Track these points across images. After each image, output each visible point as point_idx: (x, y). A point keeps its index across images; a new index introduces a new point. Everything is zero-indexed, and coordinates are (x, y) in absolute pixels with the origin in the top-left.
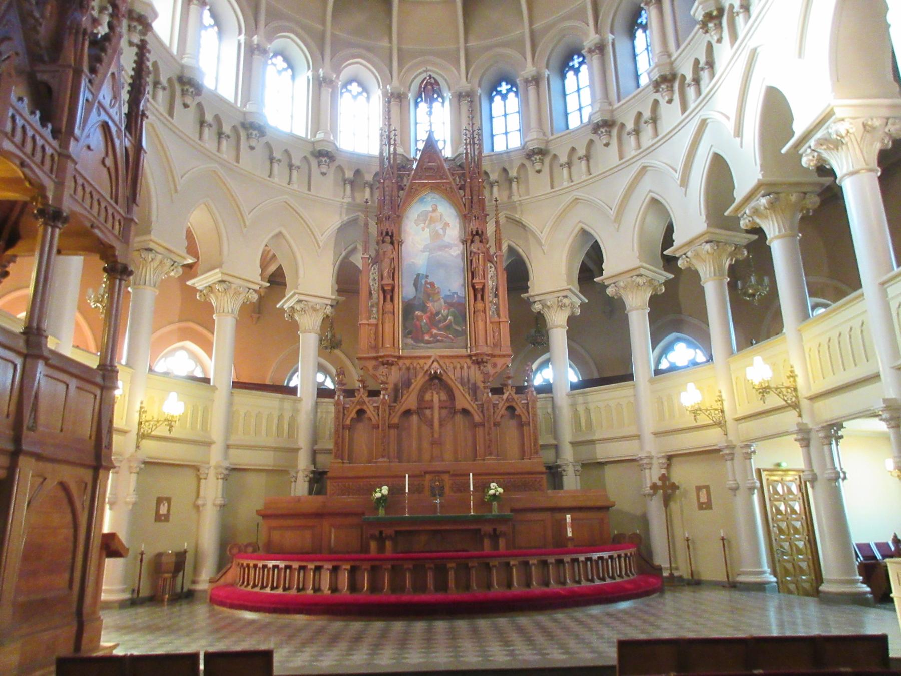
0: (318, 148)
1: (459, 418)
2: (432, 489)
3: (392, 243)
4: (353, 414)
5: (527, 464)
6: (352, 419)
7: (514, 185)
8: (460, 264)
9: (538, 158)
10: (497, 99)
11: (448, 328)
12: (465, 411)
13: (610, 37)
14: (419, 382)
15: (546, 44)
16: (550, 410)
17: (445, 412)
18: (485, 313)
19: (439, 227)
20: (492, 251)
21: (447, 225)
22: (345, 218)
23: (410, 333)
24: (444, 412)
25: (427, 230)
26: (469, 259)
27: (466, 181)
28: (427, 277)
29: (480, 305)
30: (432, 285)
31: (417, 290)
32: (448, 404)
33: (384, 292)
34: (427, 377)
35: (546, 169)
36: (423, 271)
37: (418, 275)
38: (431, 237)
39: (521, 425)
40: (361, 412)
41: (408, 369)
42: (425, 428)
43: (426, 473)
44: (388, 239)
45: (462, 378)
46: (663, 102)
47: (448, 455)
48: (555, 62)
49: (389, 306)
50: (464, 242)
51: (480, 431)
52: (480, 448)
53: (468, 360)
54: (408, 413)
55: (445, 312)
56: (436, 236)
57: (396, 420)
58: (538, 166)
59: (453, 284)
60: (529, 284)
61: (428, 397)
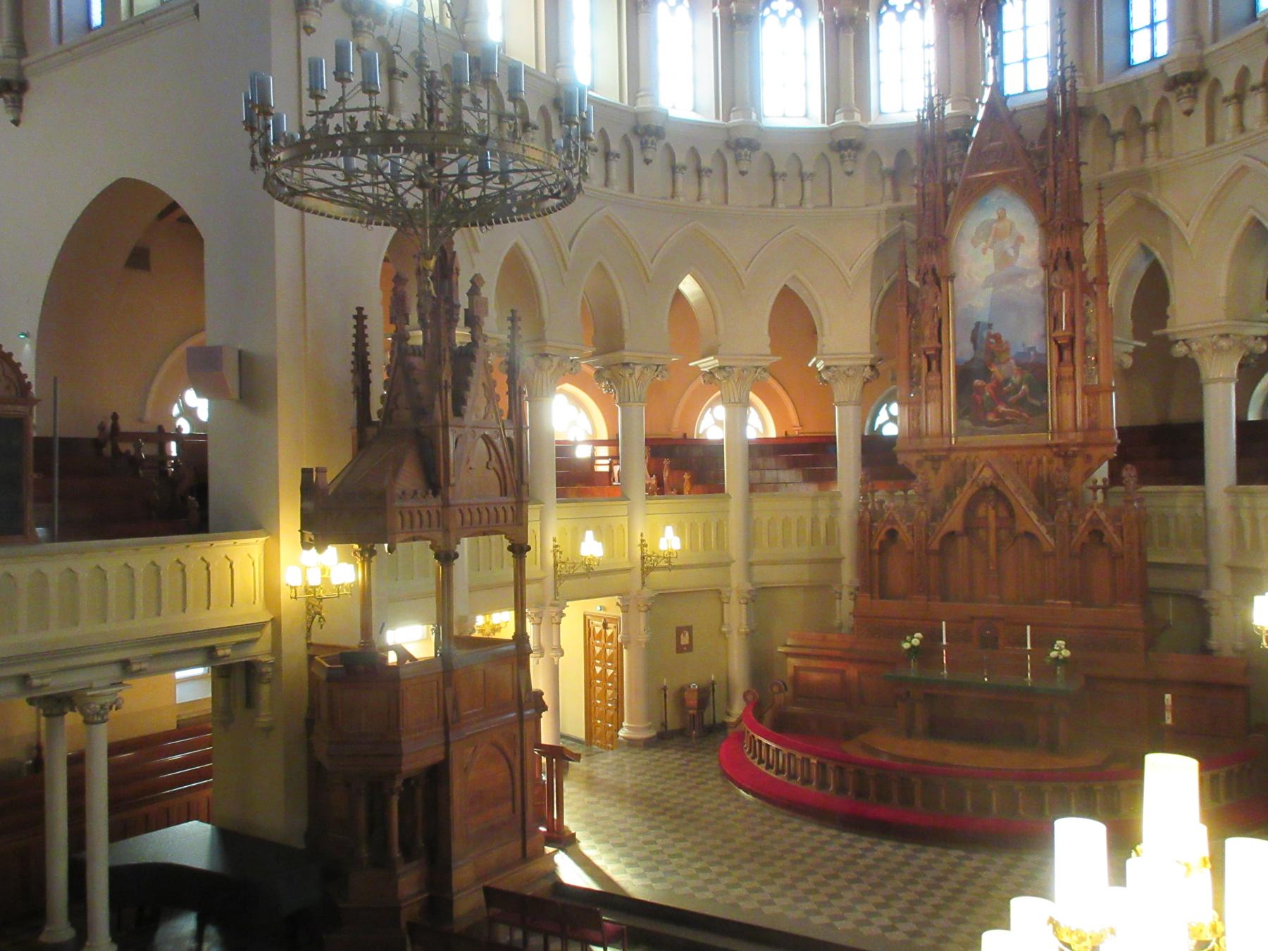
4: (882, 536)
6: (881, 543)
7: (1150, 137)
8: (1040, 299)
9: (1184, 89)
11: (1021, 402)
12: (1028, 535)
16: (1200, 512)
17: (1003, 533)
18: (1074, 378)
19: (1008, 245)
21: (1020, 239)
25: (990, 252)
26: (1050, 292)
28: (990, 326)
29: (1067, 371)
30: (997, 338)
31: (975, 348)
33: (928, 357)
34: (975, 489)
35: (1201, 107)
36: (984, 319)
37: (978, 324)
38: (997, 261)
41: (965, 464)
43: (973, 618)
44: (930, 278)
50: (1045, 266)
53: (1048, 451)
54: (951, 535)
55: (1016, 379)
56: (1003, 260)
58: (1186, 105)
59: (1026, 335)
60: (1169, 312)
61: (981, 511)
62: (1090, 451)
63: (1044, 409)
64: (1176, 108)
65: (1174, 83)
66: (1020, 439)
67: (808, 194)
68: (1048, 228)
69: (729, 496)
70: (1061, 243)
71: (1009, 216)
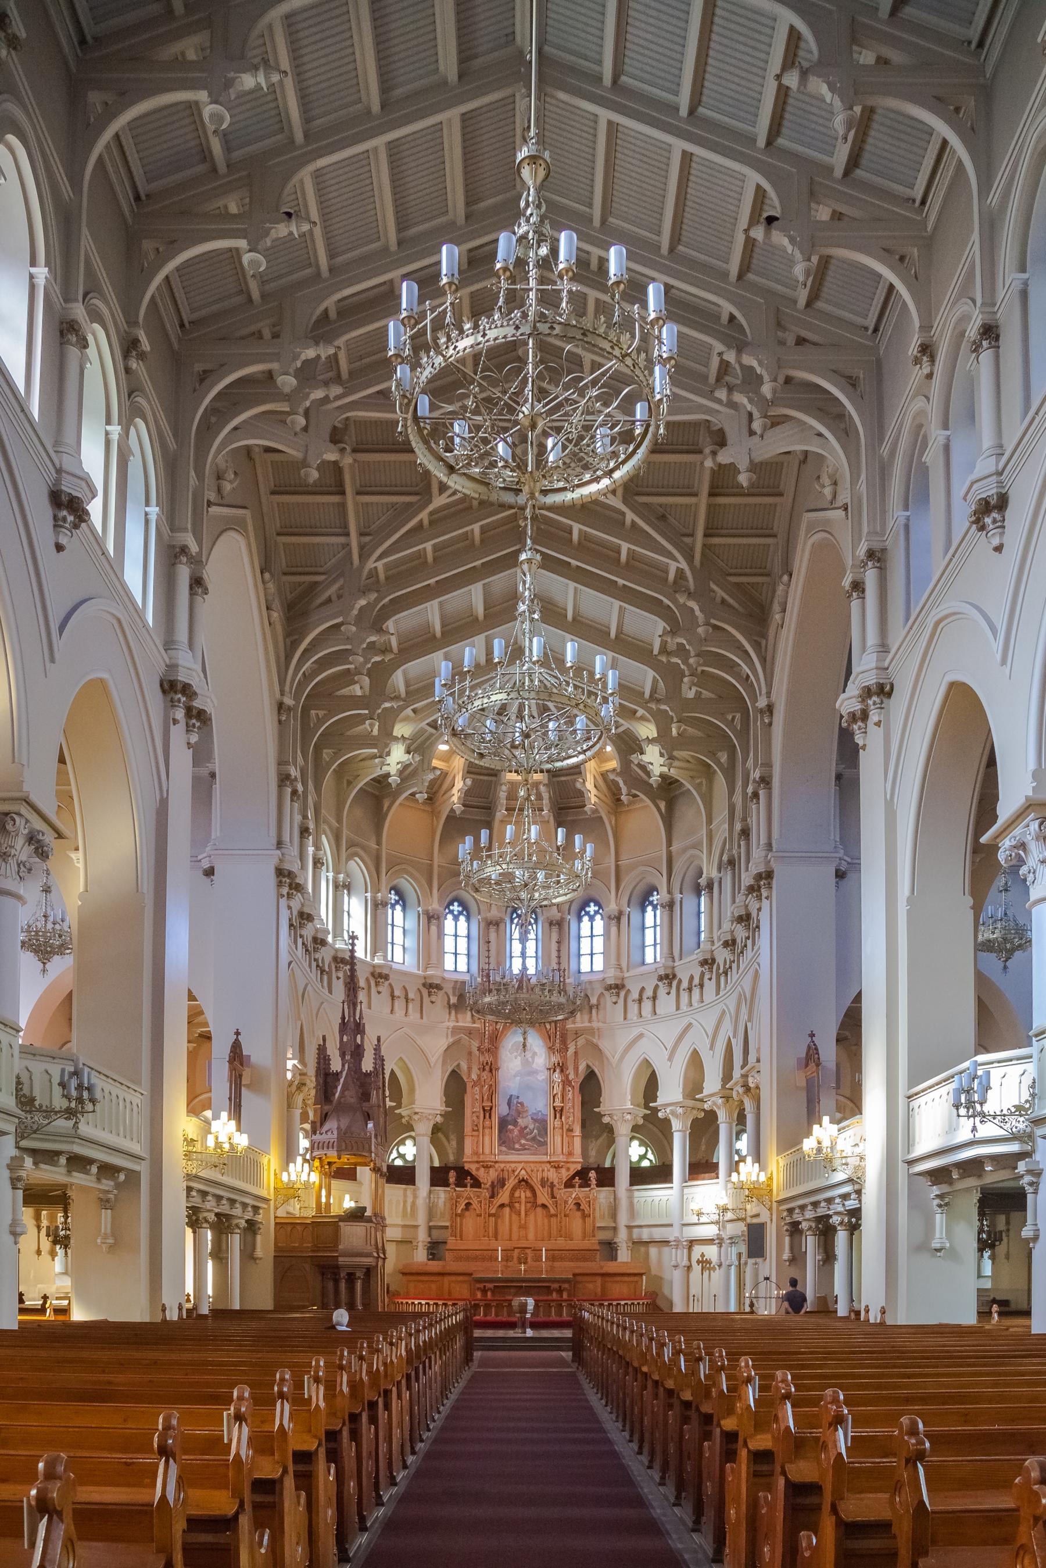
0: (429, 981)
1: (539, 1210)
2: (519, 1259)
3: (491, 1071)
4: (463, 1206)
5: (586, 1244)
10: (586, 919)
11: (534, 1139)
12: (544, 1206)
14: (511, 1183)
15: (629, 881)
20: (571, 1077)
21: (535, 1054)
22: (451, 1040)
23: (504, 1142)
24: (529, 1205)
27: (553, 1008)
30: (522, 1104)
32: (532, 1200)
35: (621, 1001)
36: (515, 1093)
39: (584, 1216)
40: (468, 1205)
42: (514, 1216)
45: (543, 1178)
46: (707, 976)
47: (531, 1236)
49: (487, 1123)
51: (553, 1220)
52: (554, 1232)
54: (502, 1206)
55: (531, 1127)
56: (526, 1063)
57: (493, 1211)
58: (614, 999)
59: (539, 1104)
61: (517, 1194)
62: (568, 1165)
63: (545, 1143)
64: (609, 998)
65: (609, 988)
69: (361, 1184)
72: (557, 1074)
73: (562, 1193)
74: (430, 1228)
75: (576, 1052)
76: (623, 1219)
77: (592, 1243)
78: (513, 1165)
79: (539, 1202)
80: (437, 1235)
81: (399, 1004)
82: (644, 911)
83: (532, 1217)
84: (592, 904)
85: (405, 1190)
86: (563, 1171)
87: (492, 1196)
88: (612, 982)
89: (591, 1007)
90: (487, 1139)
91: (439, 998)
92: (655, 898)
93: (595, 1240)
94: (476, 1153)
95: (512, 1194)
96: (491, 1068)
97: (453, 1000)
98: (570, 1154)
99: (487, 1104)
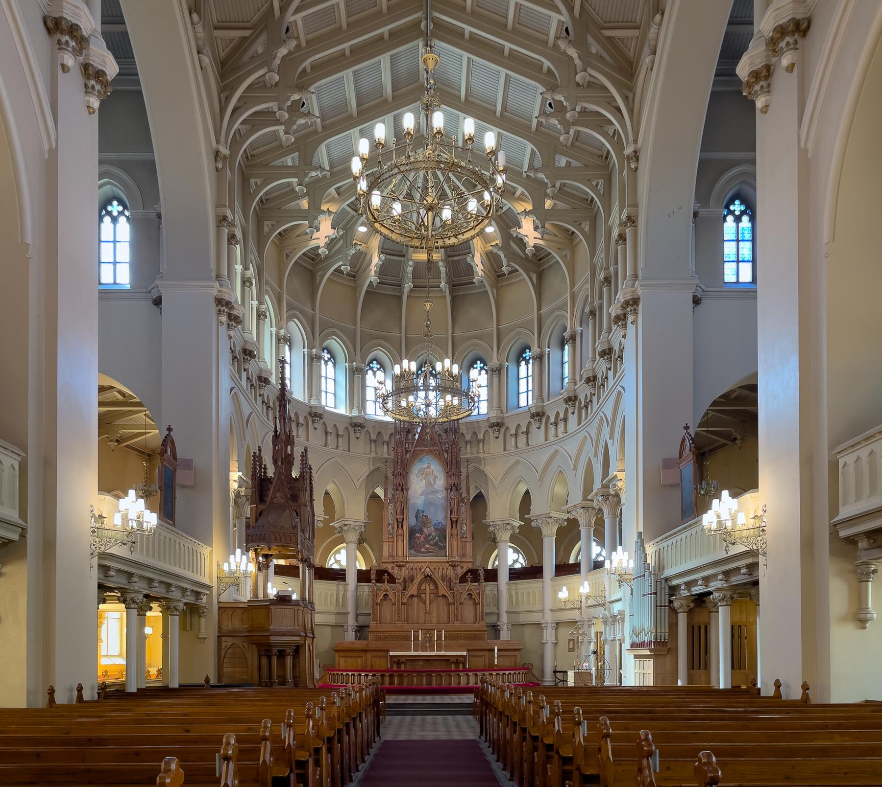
1: (440, 599)
4: (382, 597)
5: (477, 626)
11: (436, 544)
13: (547, 350)
14: (419, 578)
17: (432, 596)
20: (464, 495)
21: (436, 477)
24: (432, 596)
27: (448, 441)
29: (454, 532)
32: (435, 591)
39: (475, 604)
40: (386, 595)
42: (421, 604)
47: (434, 620)
48: (513, 355)
51: (452, 607)
52: (452, 617)
53: (447, 565)
54: (412, 596)
55: (434, 534)
56: (429, 484)
57: (405, 601)
59: (439, 516)
61: (423, 587)
64: (492, 434)
65: (492, 426)
66: (435, 559)
67: (340, 444)
68: (449, 474)
70: (454, 480)
71: (432, 467)
72: (453, 493)
73: (459, 587)
74: (357, 615)
75: (468, 477)
76: (504, 607)
77: (481, 625)
78: (420, 565)
79: (440, 594)
80: (362, 620)
81: (331, 439)
82: (519, 365)
83: (434, 605)
84: (478, 362)
85: (338, 585)
86: (459, 568)
87: (404, 589)
88: (494, 421)
89: (479, 441)
90: (400, 543)
91: (362, 435)
92: (528, 354)
93: (483, 623)
94: (391, 556)
95: (419, 588)
96: (402, 488)
97: (373, 437)
98: (464, 555)
99: (400, 516)
